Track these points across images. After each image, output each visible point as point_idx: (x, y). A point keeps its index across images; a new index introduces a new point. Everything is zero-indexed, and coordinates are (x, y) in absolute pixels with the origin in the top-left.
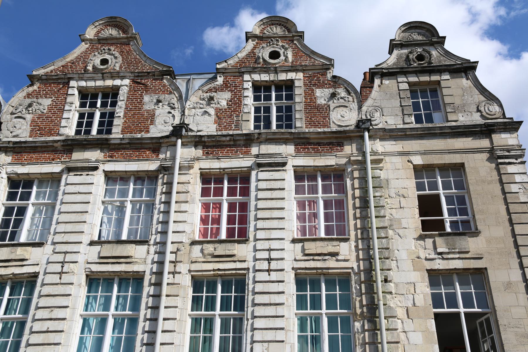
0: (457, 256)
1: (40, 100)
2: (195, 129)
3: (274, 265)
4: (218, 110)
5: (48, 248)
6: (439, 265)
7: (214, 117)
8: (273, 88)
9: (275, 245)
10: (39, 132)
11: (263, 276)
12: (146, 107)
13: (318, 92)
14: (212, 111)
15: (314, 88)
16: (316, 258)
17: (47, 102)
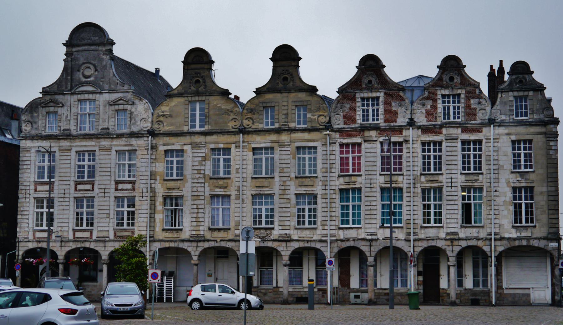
0: (524, 181)
1: (344, 105)
2: (417, 121)
3: (453, 184)
4: (426, 110)
5: (363, 177)
6: (517, 185)
7: (425, 114)
8: (451, 97)
9: (453, 176)
10: (348, 122)
11: (450, 189)
12: (394, 109)
13: (472, 101)
14: (424, 111)
15: (470, 98)
16: (470, 181)
17: (348, 106)
